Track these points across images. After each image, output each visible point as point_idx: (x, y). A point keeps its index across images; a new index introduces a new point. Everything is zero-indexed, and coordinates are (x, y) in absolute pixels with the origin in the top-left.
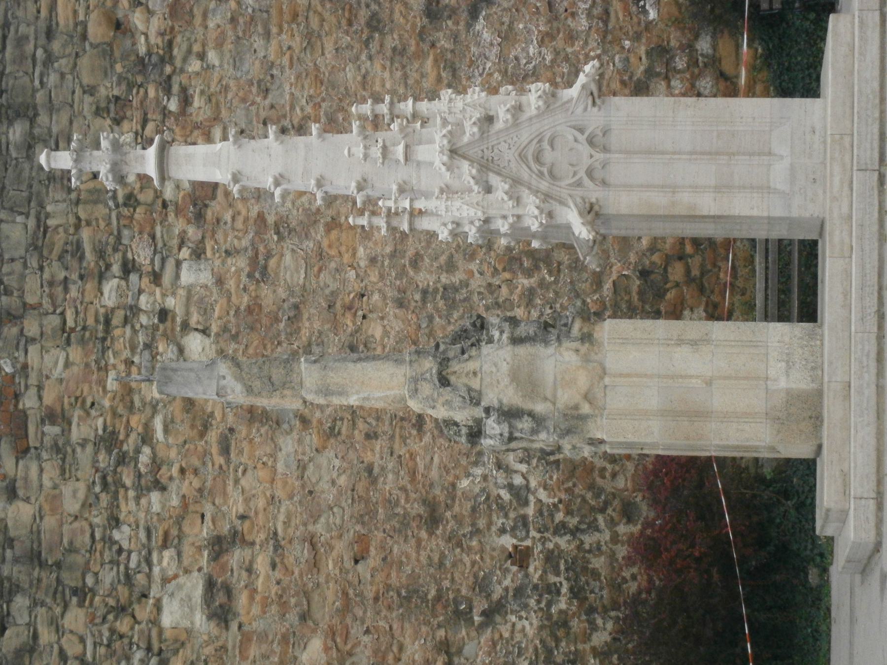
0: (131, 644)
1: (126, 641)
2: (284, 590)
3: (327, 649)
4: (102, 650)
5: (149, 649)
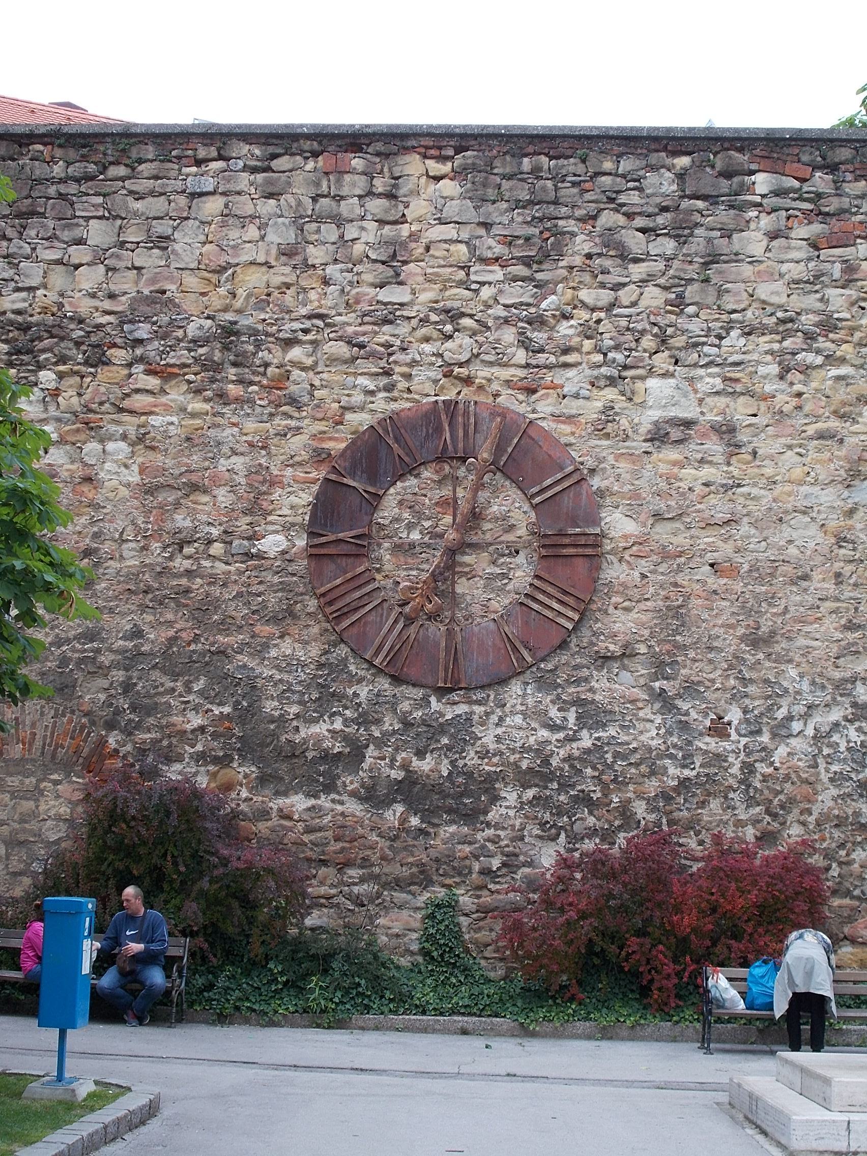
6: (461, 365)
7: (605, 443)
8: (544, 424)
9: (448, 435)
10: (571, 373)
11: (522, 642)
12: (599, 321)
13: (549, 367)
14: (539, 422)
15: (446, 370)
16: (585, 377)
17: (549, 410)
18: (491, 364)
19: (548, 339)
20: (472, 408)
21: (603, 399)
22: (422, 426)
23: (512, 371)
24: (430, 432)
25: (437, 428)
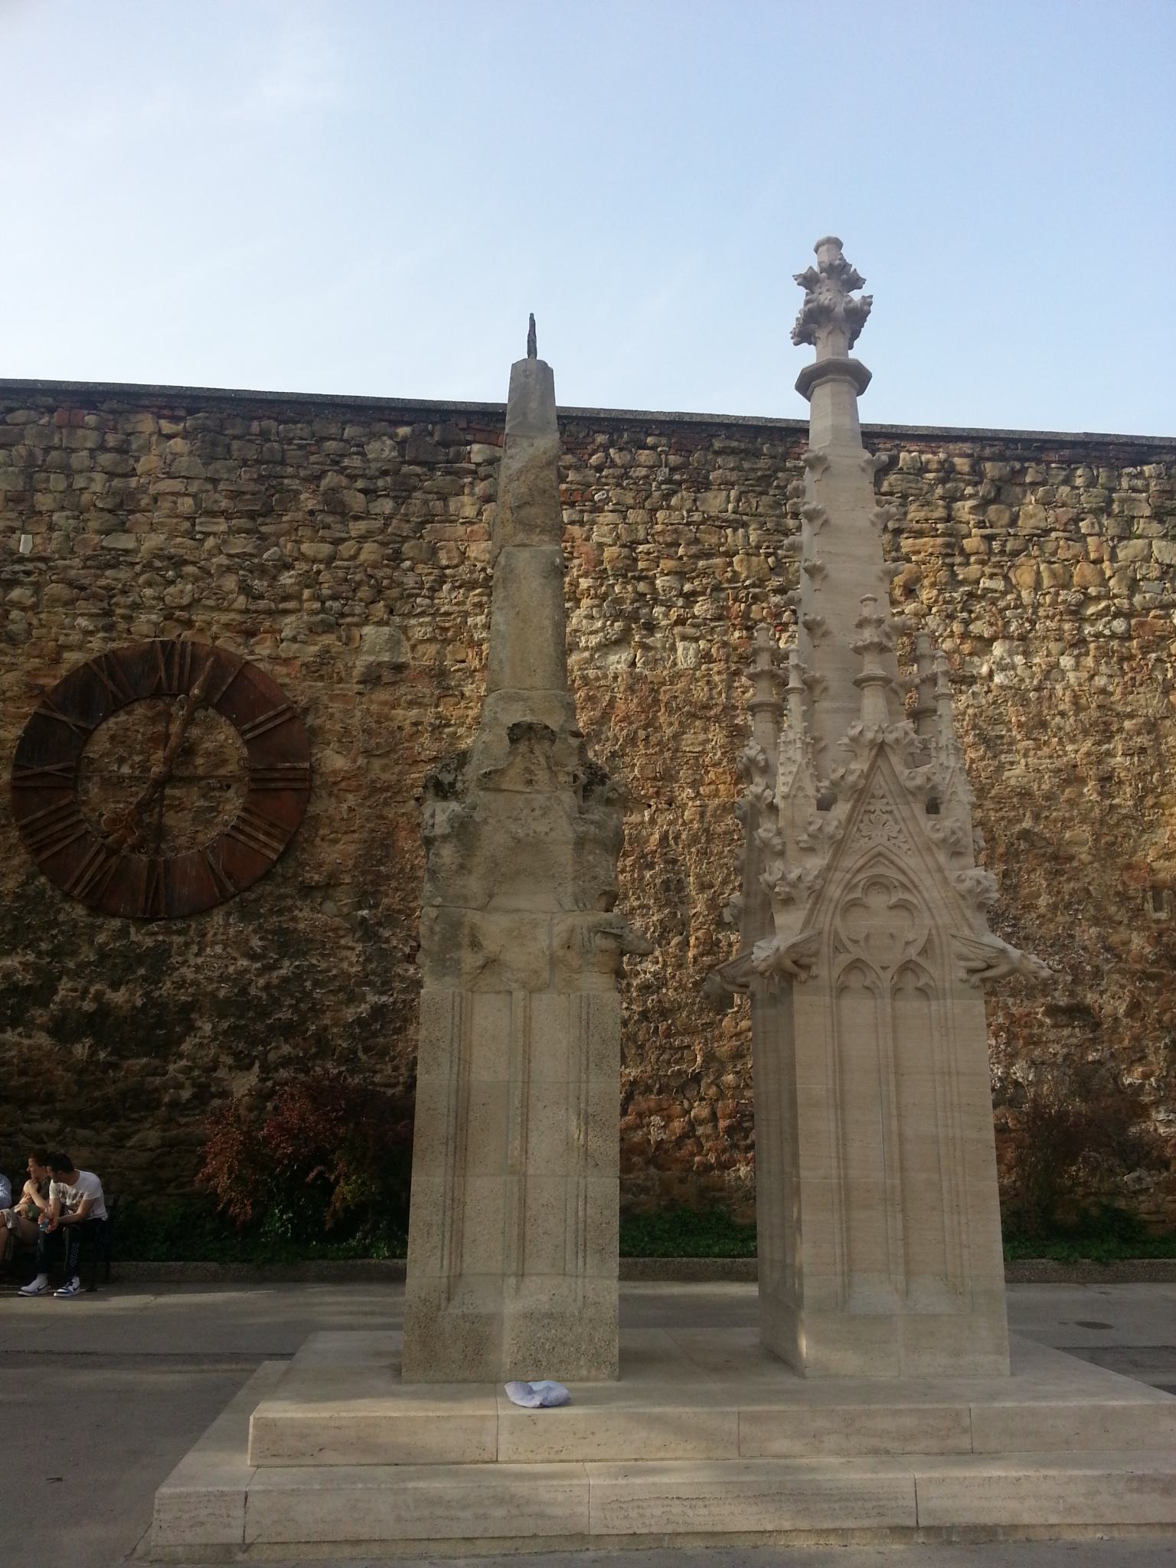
0: (347, 599)
1: (350, 594)
2: (392, 733)
3: (335, 772)
4: (341, 574)
5: (343, 615)
6: (182, 608)
8: (261, 665)
9: (163, 674)
10: (290, 619)
12: (319, 572)
13: (270, 613)
14: (255, 663)
17: (266, 652)
18: (211, 608)
20: (189, 649)
23: (232, 615)
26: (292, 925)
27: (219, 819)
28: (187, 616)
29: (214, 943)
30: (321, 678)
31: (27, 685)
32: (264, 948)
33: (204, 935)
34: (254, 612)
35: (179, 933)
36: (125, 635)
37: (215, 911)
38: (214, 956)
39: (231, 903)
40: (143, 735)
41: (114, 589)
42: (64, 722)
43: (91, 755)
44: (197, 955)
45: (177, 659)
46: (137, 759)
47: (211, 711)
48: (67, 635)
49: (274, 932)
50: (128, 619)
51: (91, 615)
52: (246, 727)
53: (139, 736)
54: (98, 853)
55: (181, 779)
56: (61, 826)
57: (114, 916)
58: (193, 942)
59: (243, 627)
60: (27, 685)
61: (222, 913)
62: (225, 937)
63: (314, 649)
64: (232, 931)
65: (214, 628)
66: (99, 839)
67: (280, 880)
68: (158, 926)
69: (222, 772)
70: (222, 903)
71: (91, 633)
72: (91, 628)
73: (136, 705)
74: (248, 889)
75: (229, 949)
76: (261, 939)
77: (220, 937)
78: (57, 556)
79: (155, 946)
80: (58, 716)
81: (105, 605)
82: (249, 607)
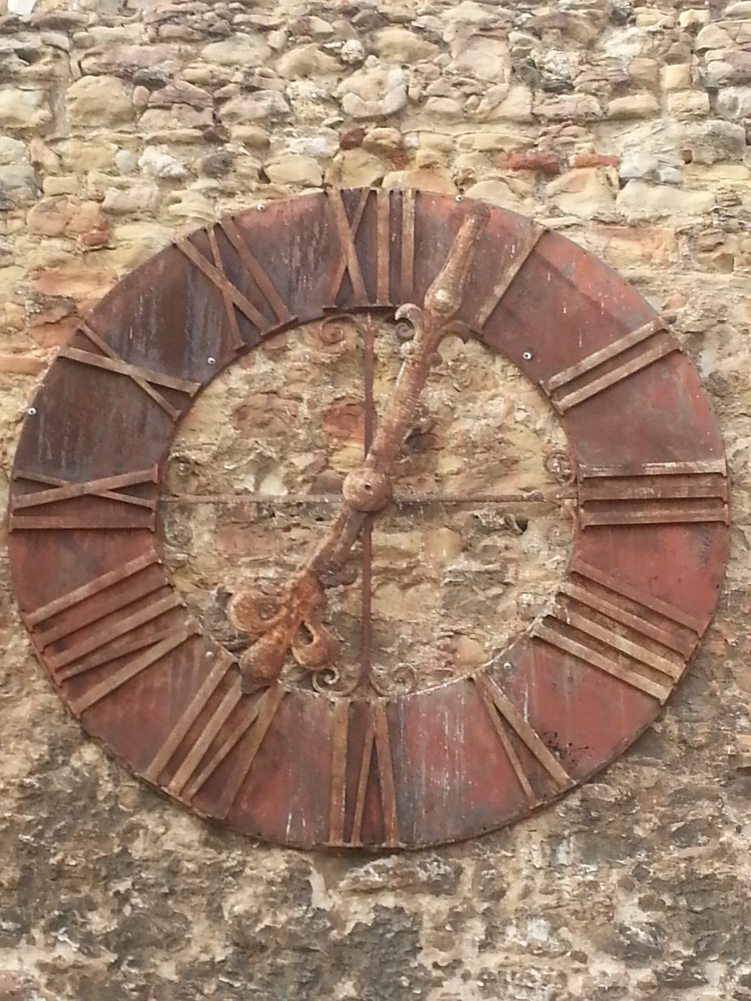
6: (382, 120)
7: (724, 278)
8: (578, 238)
9: (352, 262)
10: (636, 133)
11: (543, 734)
12: (694, 28)
13: (588, 121)
14: (566, 234)
15: (344, 130)
16: (670, 140)
17: (588, 210)
18: (449, 117)
19: (581, 63)
20: (409, 205)
21: (713, 188)
22: (292, 244)
23: (501, 130)
24: (311, 256)
25: (327, 250)
26: (720, 869)
27: (508, 603)
28: (396, 136)
29: (525, 915)
30: (727, 262)
31: (37, 298)
32: (656, 929)
33: (500, 894)
34: (551, 121)
35: (435, 888)
36: (254, 185)
37: (521, 832)
38: (529, 950)
39: (560, 810)
40: (312, 405)
41: (223, 83)
42: (128, 377)
43: (193, 455)
44: (484, 946)
45: (382, 228)
46: (301, 461)
47: (472, 349)
48: (122, 187)
49: (678, 888)
50: (261, 147)
51: (178, 142)
52: (561, 377)
53: (304, 409)
54: (222, 687)
55: (409, 508)
56: (128, 622)
57: (266, 845)
58: (471, 913)
59: (530, 154)
60: (37, 298)
61: (537, 837)
62: (551, 900)
63: (703, 199)
64: (567, 884)
65: (462, 161)
66: (225, 654)
67: (675, 751)
68: (380, 870)
69: (506, 488)
70: (537, 812)
71: (177, 181)
72: (177, 169)
73: (291, 336)
74: (599, 775)
75: (564, 932)
76: (644, 904)
77: (539, 900)
78: (92, 17)
79: (377, 924)
80: (111, 363)
81: (206, 118)
82: (540, 110)
